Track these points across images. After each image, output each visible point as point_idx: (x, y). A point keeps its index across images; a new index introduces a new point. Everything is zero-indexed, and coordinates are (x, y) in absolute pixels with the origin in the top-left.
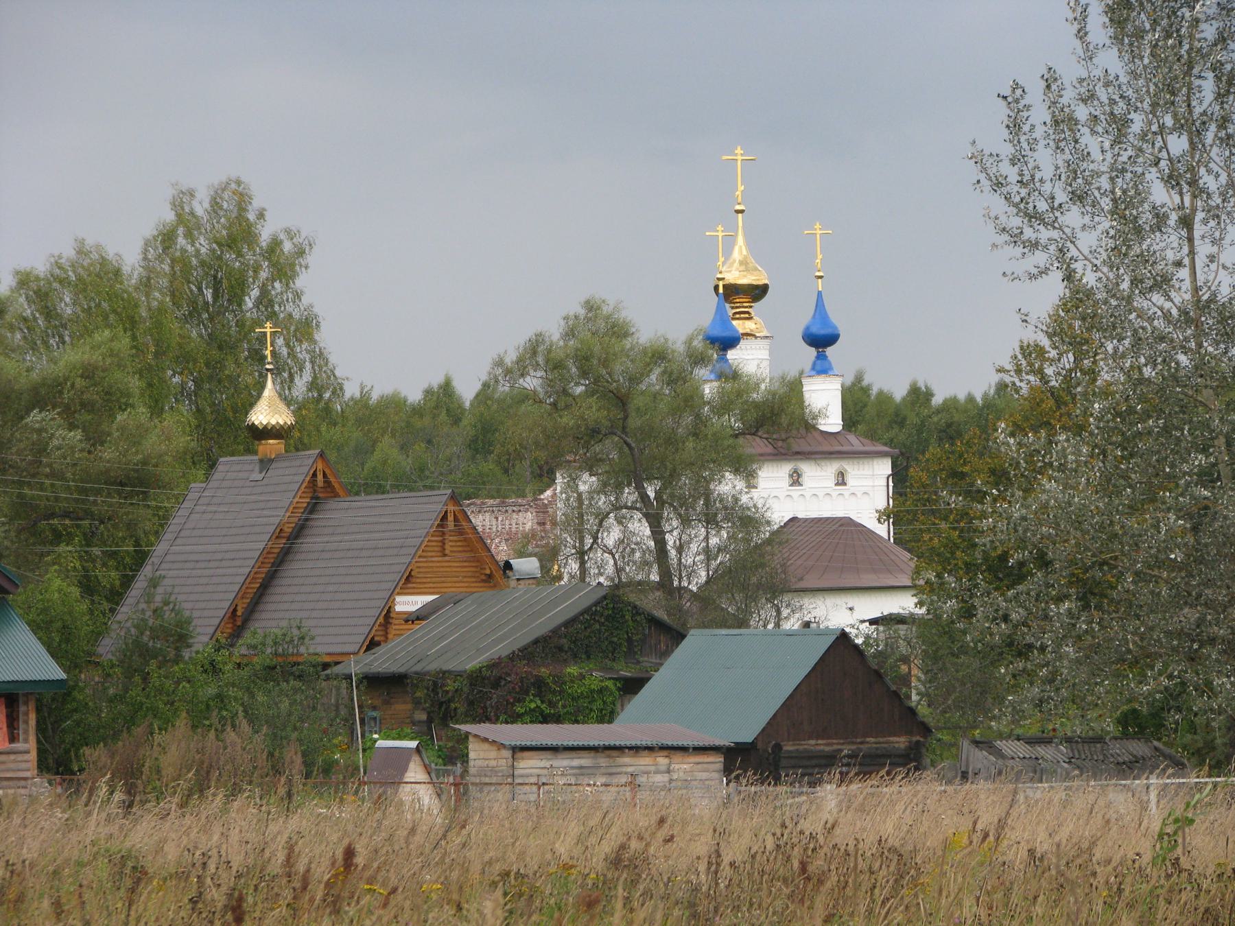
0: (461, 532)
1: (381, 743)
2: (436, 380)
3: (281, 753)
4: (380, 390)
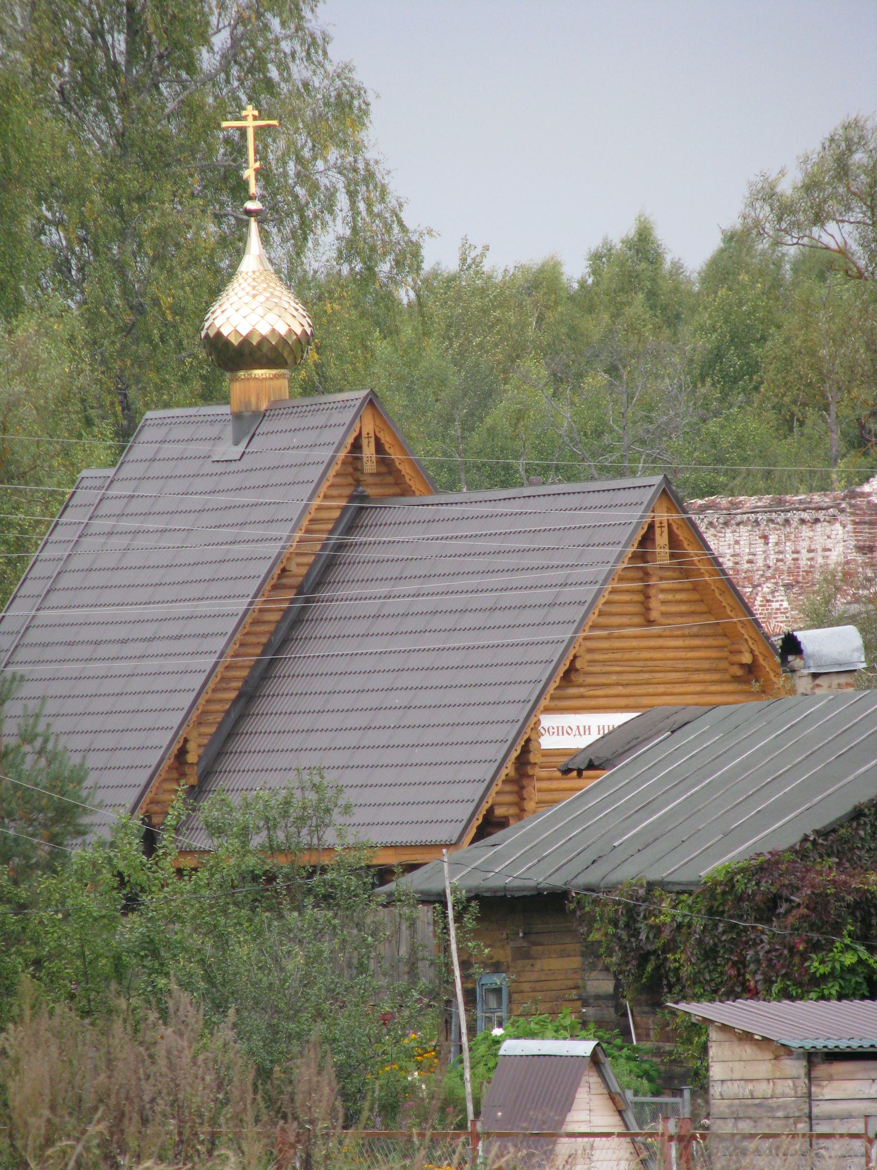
0: (684, 570)
1: (512, 1047)
2: (619, 231)
3: (287, 1071)
4: (507, 256)
